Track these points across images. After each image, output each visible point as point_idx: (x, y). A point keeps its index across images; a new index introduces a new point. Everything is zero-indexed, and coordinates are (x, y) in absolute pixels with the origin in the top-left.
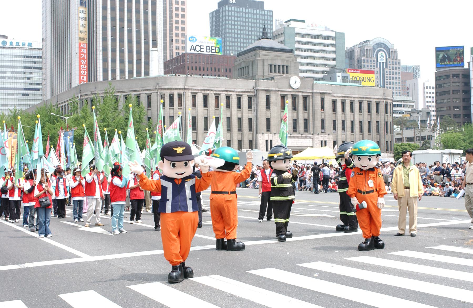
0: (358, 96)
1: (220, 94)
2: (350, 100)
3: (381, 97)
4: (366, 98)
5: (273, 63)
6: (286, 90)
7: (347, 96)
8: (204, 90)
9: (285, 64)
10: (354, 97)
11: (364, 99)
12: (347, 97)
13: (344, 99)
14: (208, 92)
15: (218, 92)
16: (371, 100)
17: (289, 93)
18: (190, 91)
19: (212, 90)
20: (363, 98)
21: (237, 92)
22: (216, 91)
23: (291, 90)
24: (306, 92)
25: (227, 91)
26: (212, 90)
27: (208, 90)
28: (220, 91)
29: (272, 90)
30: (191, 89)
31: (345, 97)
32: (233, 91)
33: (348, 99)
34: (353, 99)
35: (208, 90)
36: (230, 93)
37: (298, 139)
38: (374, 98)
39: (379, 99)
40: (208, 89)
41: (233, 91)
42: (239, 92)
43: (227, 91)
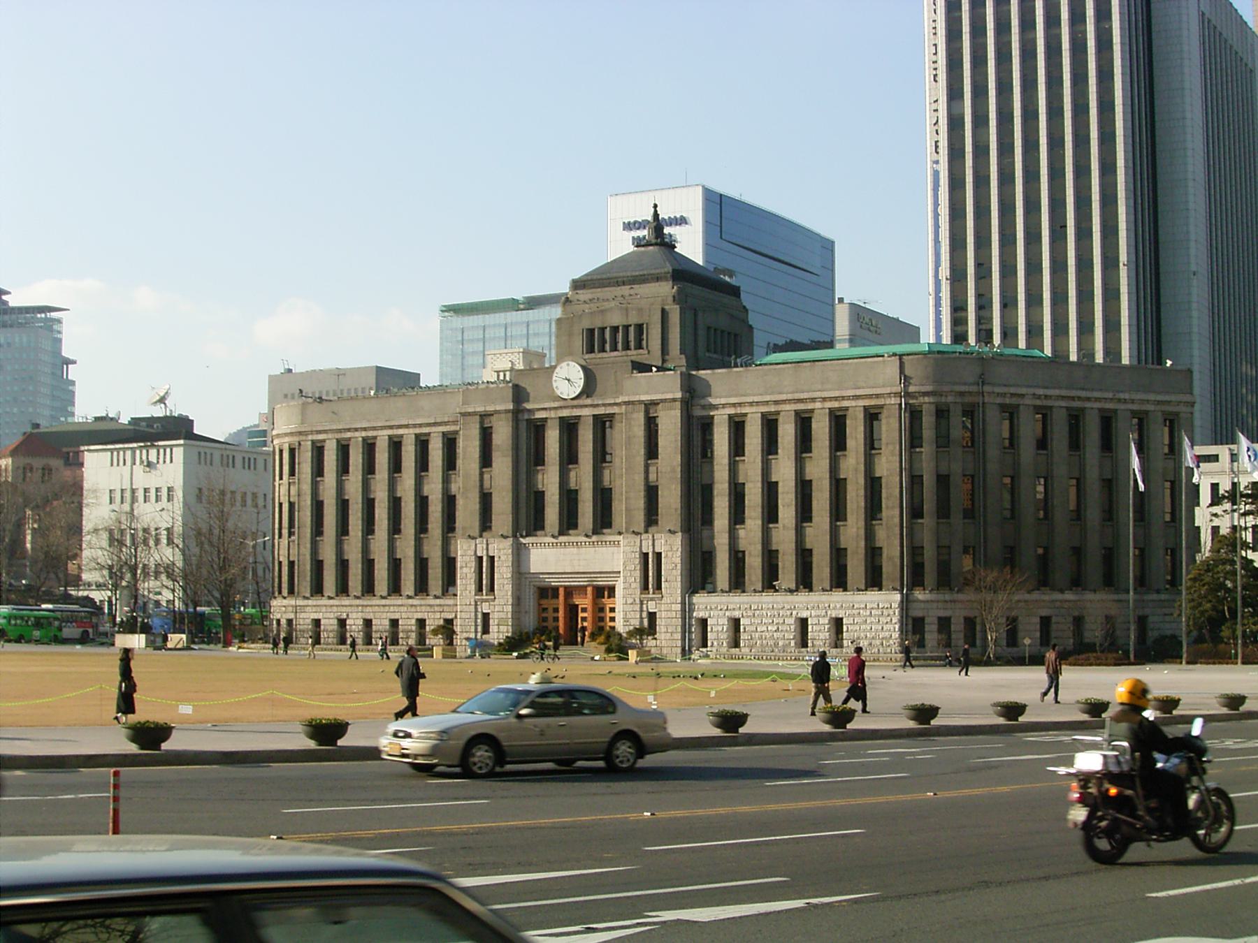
0: (790, 396)
1: (375, 438)
2: (763, 415)
3: (888, 390)
4: (824, 399)
5: (597, 323)
6: (542, 406)
7: (750, 399)
8: (340, 431)
9: (633, 319)
10: (776, 402)
11: (818, 405)
12: (751, 404)
13: (739, 410)
14: (348, 435)
15: (371, 434)
16: (845, 404)
17: (553, 414)
18: (310, 437)
19: (356, 430)
20: (813, 400)
21: (415, 426)
22: (365, 429)
23: (556, 404)
24: (604, 405)
25: (391, 427)
26: (356, 430)
27: (349, 430)
28: (374, 428)
29: (497, 412)
30: (312, 432)
31: (740, 404)
32: (407, 426)
33: (754, 409)
34: (773, 408)
35: (349, 430)
36: (401, 432)
37: (575, 550)
38: (857, 397)
39: (878, 396)
40: (348, 427)
41: (407, 426)
42: (420, 425)
43: (391, 427)
